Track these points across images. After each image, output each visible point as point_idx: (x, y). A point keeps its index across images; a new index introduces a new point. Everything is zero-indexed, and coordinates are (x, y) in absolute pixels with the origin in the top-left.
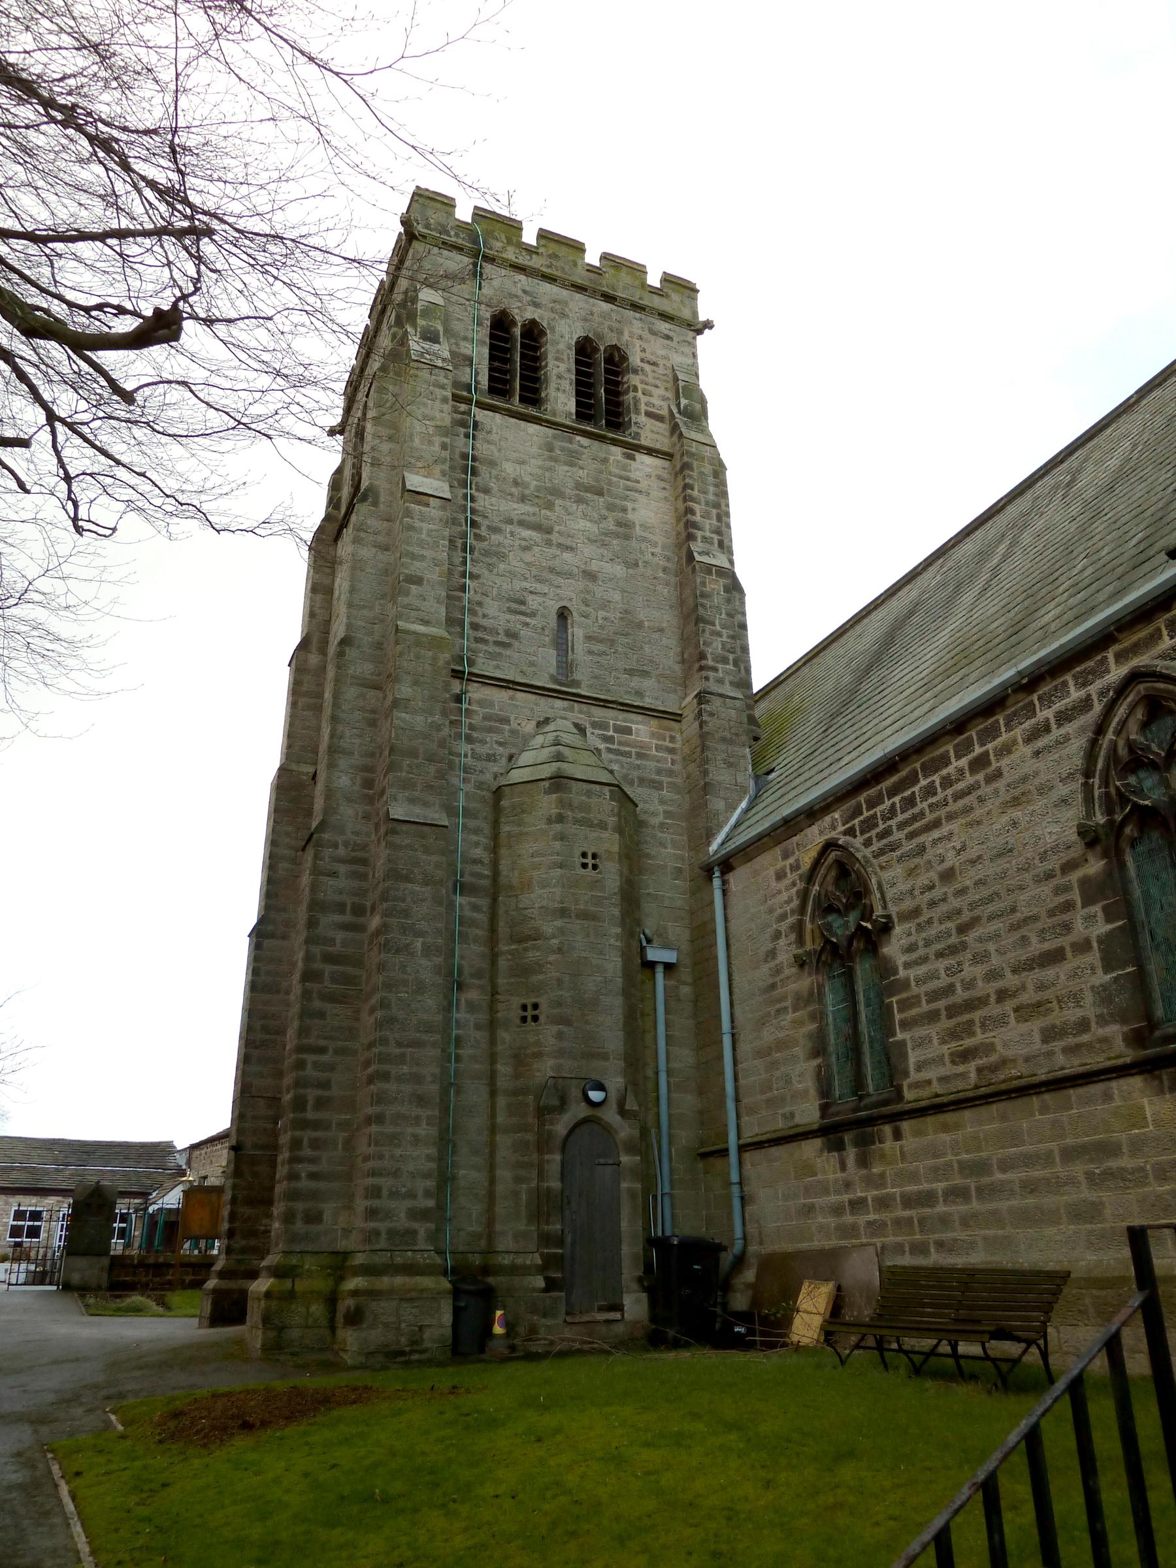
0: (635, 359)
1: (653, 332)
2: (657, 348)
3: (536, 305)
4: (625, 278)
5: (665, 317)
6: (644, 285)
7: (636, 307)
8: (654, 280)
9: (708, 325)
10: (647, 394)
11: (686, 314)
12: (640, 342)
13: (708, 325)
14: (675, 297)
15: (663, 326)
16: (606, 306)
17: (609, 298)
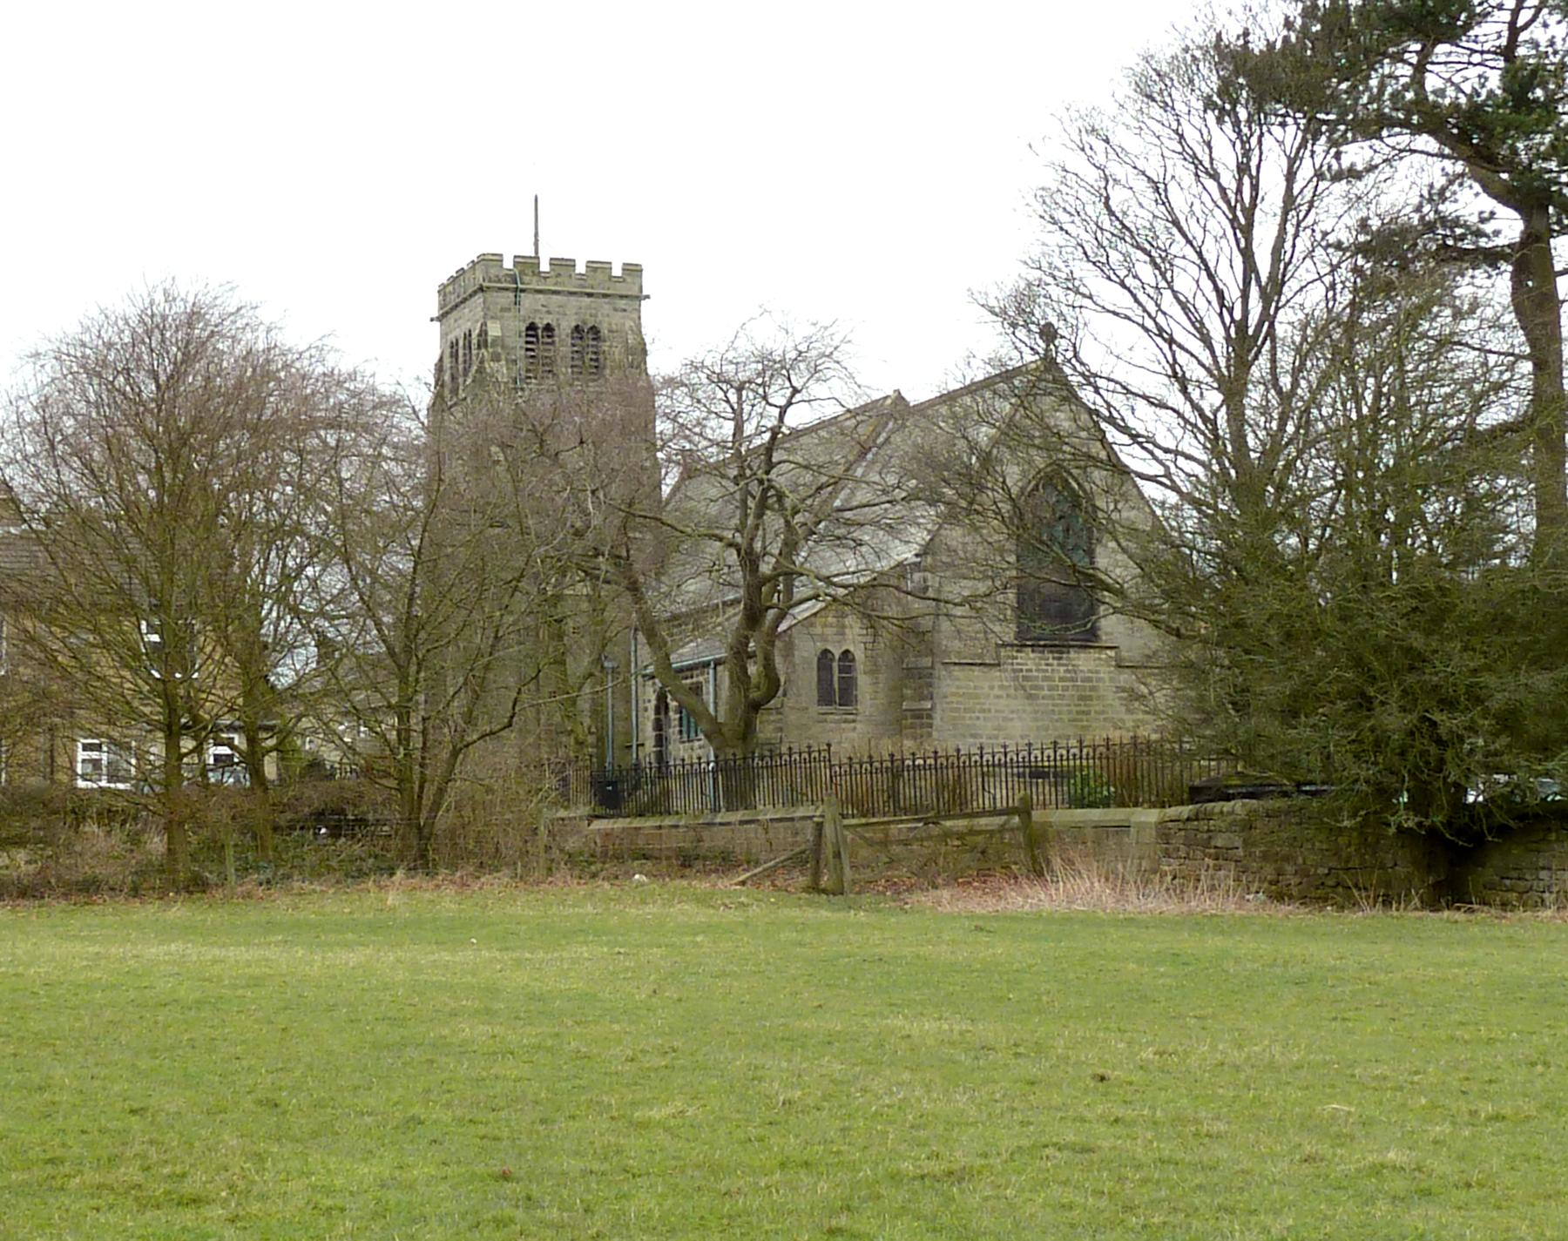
0: (604, 332)
1: (615, 310)
2: (617, 318)
3: (549, 312)
4: (599, 275)
5: (622, 297)
6: (611, 277)
7: (605, 296)
8: (617, 271)
9: (648, 297)
10: (613, 350)
11: (635, 292)
12: (607, 317)
13: (648, 297)
14: (629, 279)
15: (622, 303)
16: (588, 300)
17: (590, 295)
